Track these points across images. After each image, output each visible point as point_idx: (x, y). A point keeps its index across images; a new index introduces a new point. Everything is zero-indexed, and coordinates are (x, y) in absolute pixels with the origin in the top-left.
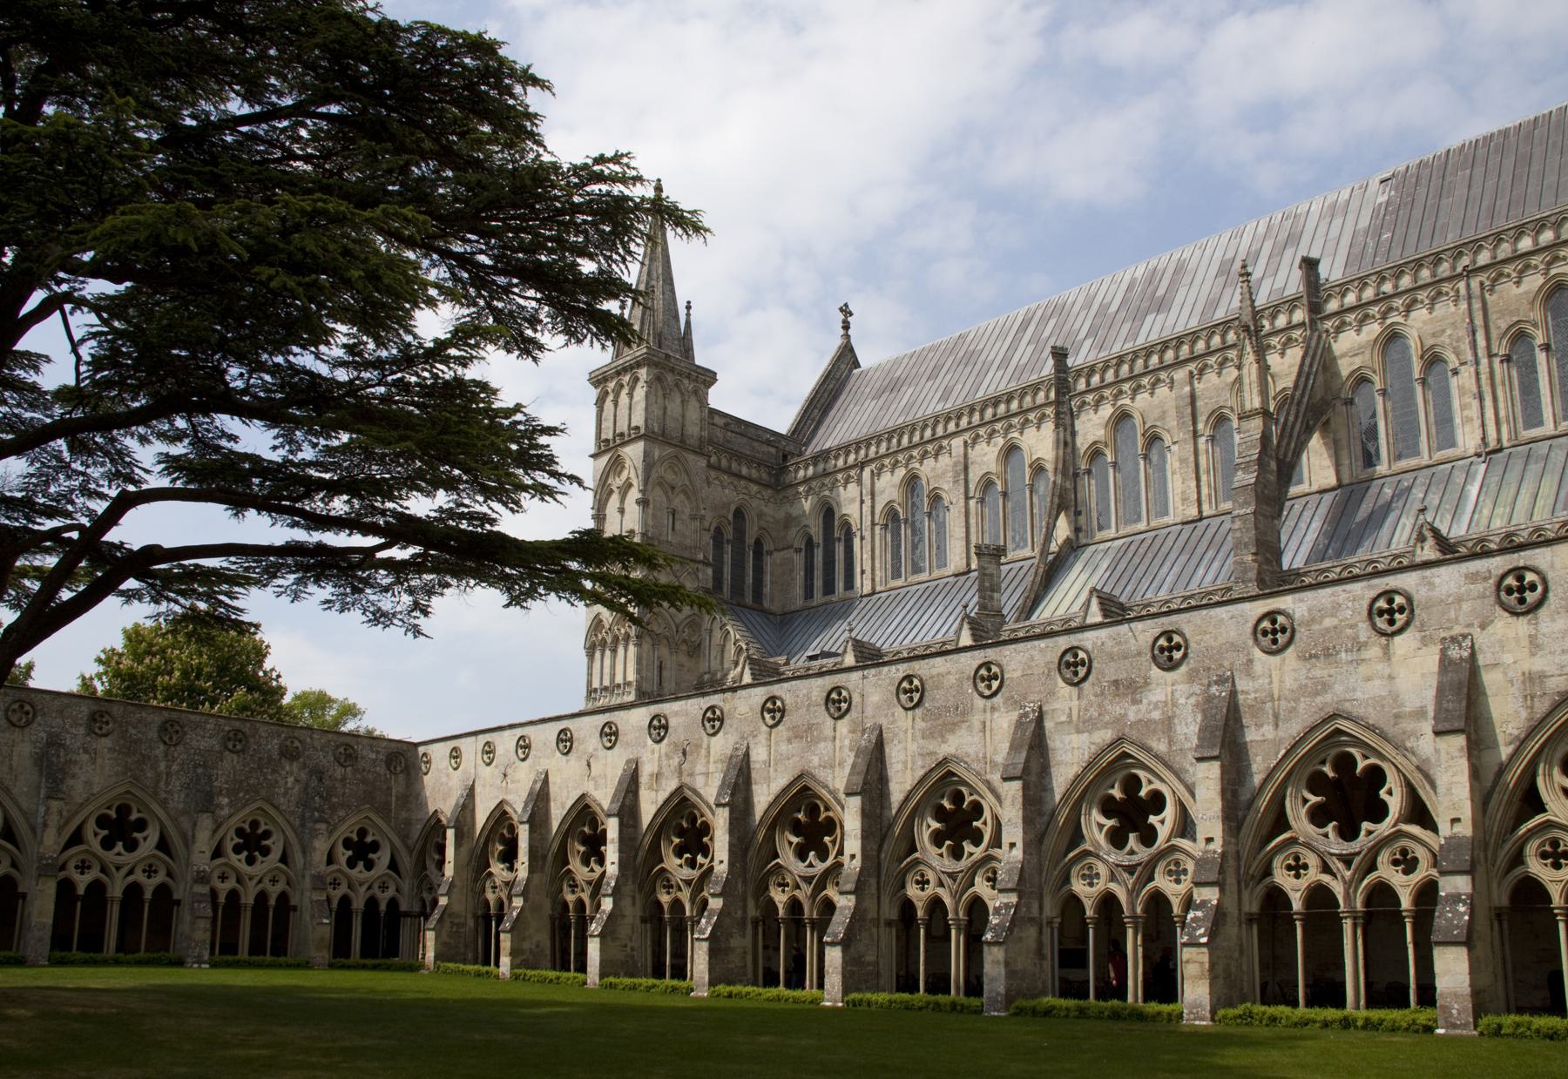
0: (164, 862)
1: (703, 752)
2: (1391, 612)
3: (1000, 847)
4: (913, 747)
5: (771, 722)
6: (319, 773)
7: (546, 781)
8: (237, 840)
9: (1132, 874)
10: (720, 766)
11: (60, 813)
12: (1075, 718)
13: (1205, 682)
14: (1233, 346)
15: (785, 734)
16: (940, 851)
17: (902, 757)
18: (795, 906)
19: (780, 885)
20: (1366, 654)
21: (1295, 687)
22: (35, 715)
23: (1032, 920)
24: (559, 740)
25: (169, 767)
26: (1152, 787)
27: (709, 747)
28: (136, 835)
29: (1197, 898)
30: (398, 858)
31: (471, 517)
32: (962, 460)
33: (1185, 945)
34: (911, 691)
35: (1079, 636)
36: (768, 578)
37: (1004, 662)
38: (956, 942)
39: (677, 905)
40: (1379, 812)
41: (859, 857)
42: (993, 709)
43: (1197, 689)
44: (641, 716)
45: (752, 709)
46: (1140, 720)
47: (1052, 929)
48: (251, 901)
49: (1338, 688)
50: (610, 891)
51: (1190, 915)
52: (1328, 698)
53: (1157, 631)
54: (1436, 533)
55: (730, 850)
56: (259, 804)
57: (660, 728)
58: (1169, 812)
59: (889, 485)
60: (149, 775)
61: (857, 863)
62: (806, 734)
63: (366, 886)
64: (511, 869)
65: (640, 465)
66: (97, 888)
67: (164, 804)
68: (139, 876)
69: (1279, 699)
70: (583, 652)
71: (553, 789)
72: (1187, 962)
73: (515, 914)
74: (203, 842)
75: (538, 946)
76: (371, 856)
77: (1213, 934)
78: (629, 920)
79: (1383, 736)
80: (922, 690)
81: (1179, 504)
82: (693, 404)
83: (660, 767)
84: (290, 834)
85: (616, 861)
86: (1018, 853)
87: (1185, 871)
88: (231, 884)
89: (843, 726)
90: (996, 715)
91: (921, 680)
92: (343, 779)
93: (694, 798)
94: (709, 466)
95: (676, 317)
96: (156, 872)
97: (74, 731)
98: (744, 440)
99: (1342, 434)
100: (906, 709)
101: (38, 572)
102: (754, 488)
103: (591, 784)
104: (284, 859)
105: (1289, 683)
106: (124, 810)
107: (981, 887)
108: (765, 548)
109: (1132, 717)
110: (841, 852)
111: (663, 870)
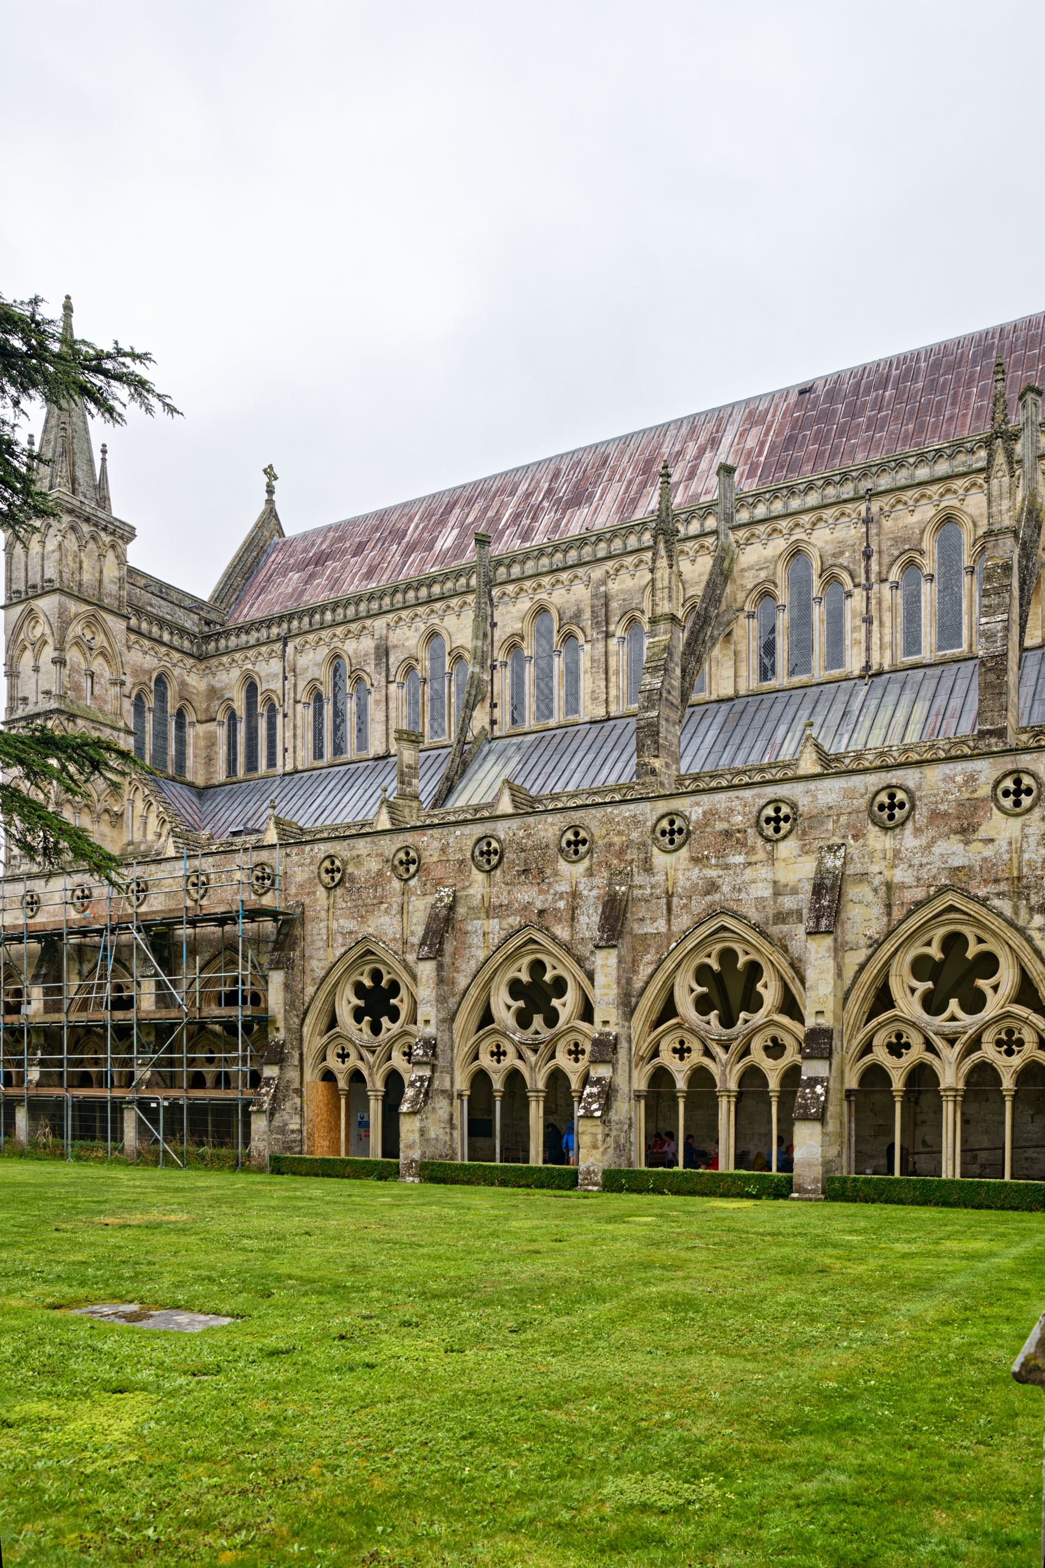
2: (777, 820)
9: (535, 1051)
14: (648, 548)
26: (555, 972)
36: (190, 751)
51: (588, 1090)
53: (564, 826)
58: (571, 996)
65: (56, 625)
77: (606, 1108)
87: (583, 1052)
99: (742, 647)
102: (176, 656)
108: (188, 720)
109: (539, 905)
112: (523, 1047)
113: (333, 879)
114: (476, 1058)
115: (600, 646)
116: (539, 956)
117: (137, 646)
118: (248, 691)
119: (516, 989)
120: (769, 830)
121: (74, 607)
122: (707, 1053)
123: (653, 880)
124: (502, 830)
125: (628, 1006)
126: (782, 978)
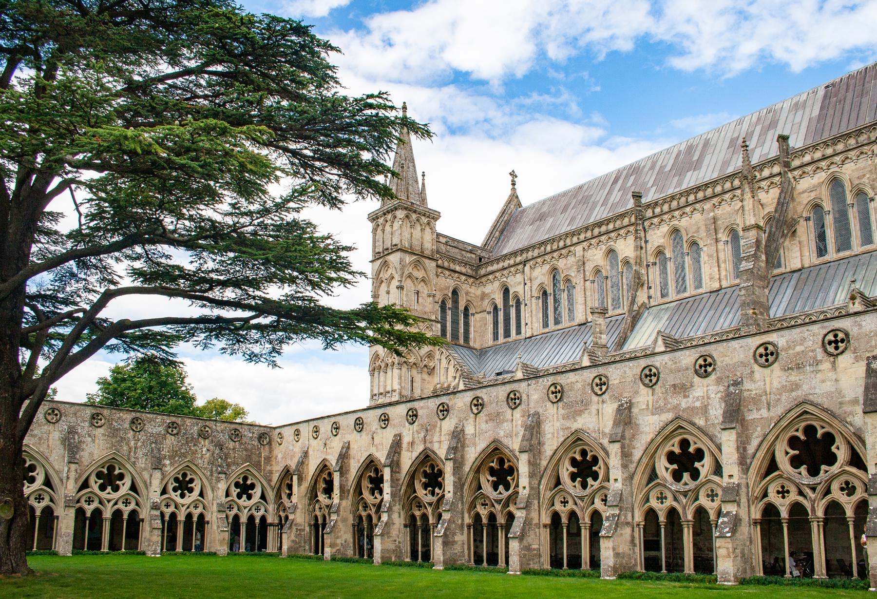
0: (135, 498)
1: (438, 429)
2: (836, 342)
3: (609, 481)
4: (557, 425)
5: (476, 411)
6: (221, 446)
7: (348, 448)
9: (685, 496)
10: (447, 437)
11: (76, 470)
12: (650, 407)
13: (726, 384)
15: (484, 418)
16: (574, 484)
17: (551, 430)
18: (492, 517)
19: (483, 505)
20: (820, 367)
21: (779, 386)
22: (61, 416)
23: (628, 523)
24: (356, 424)
25: (137, 444)
26: (696, 446)
28: (118, 482)
29: (724, 510)
31: (303, 299)
32: (582, 258)
33: (717, 537)
34: (556, 392)
35: (652, 359)
36: (472, 329)
37: (609, 375)
38: (585, 535)
39: (425, 517)
40: (831, 459)
41: (527, 488)
42: (603, 402)
43: (721, 388)
44: (402, 409)
45: (465, 405)
46: (689, 407)
47: (640, 528)
49: (805, 387)
50: (386, 510)
51: (720, 520)
52: (799, 392)
53: (698, 355)
54: (862, 295)
55: (454, 485)
57: (413, 416)
58: (707, 461)
59: (540, 274)
60: (125, 448)
61: (526, 492)
62: (496, 418)
63: (249, 508)
64: (330, 498)
65: (398, 266)
66: (97, 513)
68: (120, 506)
69: (770, 394)
70: (368, 373)
71: (352, 452)
72: (719, 547)
73: (332, 523)
75: (345, 542)
76: (250, 492)
77: (734, 531)
78: (397, 526)
79: (833, 415)
80: (561, 392)
81: (708, 281)
82: (428, 230)
83: (413, 438)
84: (204, 480)
85: (389, 492)
86: (619, 485)
87: (717, 495)
88: (172, 509)
89: (518, 413)
90: (605, 405)
91: (561, 386)
93: (433, 456)
94: (438, 266)
95: (417, 182)
96: (130, 503)
97: (82, 424)
98: (457, 250)
100: (553, 403)
101: (60, 337)
102: (464, 278)
103: (374, 448)
104: (201, 494)
105: (776, 384)
106: (111, 468)
107: (598, 504)
109: (684, 405)
110: (517, 486)
111: (416, 497)
112: (677, 494)
113: (556, 397)
114: (648, 500)
115: (714, 248)
116: (685, 436)
117: (442, 275)
118: (504, 293)
119: (671, 457)
120: (831, 349)
121: (408, 259)
122: (801, 493)
123: (757, 386)
124: (657, 361)
125: (744, 464)
126: (849, 442)
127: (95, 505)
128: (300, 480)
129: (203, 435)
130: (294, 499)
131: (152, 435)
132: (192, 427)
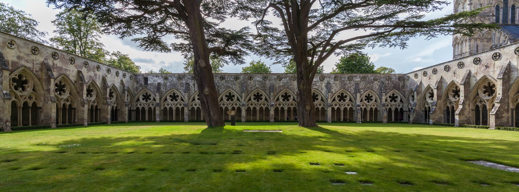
6: (383, 83)
8: (365, 98)
11: (331, 96)
27: (494, 64)
30: (402, 99)
48: (369, 110)
56: (370, 90)
63: (395, 105)
66: (338, 109)
67: (350, 92)
68: (346, 106)
74: (358, 99)
76: (396, 99)
84: (377, 96)
88: (365, 107)
92: (388, 83)
104: (376, 101)
106: (342, 94)
127: (338, 106)
128: (418, 94)
129: (375, 80)
130: (415, 101)
131: (356, 81)
132: (370, 77)
